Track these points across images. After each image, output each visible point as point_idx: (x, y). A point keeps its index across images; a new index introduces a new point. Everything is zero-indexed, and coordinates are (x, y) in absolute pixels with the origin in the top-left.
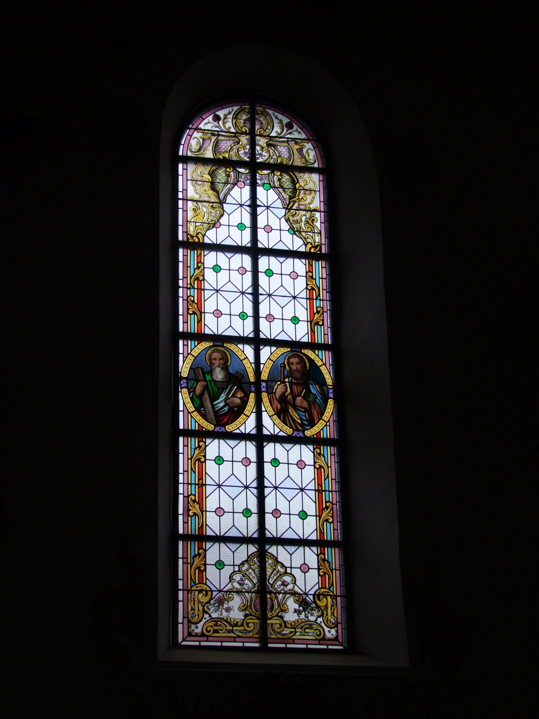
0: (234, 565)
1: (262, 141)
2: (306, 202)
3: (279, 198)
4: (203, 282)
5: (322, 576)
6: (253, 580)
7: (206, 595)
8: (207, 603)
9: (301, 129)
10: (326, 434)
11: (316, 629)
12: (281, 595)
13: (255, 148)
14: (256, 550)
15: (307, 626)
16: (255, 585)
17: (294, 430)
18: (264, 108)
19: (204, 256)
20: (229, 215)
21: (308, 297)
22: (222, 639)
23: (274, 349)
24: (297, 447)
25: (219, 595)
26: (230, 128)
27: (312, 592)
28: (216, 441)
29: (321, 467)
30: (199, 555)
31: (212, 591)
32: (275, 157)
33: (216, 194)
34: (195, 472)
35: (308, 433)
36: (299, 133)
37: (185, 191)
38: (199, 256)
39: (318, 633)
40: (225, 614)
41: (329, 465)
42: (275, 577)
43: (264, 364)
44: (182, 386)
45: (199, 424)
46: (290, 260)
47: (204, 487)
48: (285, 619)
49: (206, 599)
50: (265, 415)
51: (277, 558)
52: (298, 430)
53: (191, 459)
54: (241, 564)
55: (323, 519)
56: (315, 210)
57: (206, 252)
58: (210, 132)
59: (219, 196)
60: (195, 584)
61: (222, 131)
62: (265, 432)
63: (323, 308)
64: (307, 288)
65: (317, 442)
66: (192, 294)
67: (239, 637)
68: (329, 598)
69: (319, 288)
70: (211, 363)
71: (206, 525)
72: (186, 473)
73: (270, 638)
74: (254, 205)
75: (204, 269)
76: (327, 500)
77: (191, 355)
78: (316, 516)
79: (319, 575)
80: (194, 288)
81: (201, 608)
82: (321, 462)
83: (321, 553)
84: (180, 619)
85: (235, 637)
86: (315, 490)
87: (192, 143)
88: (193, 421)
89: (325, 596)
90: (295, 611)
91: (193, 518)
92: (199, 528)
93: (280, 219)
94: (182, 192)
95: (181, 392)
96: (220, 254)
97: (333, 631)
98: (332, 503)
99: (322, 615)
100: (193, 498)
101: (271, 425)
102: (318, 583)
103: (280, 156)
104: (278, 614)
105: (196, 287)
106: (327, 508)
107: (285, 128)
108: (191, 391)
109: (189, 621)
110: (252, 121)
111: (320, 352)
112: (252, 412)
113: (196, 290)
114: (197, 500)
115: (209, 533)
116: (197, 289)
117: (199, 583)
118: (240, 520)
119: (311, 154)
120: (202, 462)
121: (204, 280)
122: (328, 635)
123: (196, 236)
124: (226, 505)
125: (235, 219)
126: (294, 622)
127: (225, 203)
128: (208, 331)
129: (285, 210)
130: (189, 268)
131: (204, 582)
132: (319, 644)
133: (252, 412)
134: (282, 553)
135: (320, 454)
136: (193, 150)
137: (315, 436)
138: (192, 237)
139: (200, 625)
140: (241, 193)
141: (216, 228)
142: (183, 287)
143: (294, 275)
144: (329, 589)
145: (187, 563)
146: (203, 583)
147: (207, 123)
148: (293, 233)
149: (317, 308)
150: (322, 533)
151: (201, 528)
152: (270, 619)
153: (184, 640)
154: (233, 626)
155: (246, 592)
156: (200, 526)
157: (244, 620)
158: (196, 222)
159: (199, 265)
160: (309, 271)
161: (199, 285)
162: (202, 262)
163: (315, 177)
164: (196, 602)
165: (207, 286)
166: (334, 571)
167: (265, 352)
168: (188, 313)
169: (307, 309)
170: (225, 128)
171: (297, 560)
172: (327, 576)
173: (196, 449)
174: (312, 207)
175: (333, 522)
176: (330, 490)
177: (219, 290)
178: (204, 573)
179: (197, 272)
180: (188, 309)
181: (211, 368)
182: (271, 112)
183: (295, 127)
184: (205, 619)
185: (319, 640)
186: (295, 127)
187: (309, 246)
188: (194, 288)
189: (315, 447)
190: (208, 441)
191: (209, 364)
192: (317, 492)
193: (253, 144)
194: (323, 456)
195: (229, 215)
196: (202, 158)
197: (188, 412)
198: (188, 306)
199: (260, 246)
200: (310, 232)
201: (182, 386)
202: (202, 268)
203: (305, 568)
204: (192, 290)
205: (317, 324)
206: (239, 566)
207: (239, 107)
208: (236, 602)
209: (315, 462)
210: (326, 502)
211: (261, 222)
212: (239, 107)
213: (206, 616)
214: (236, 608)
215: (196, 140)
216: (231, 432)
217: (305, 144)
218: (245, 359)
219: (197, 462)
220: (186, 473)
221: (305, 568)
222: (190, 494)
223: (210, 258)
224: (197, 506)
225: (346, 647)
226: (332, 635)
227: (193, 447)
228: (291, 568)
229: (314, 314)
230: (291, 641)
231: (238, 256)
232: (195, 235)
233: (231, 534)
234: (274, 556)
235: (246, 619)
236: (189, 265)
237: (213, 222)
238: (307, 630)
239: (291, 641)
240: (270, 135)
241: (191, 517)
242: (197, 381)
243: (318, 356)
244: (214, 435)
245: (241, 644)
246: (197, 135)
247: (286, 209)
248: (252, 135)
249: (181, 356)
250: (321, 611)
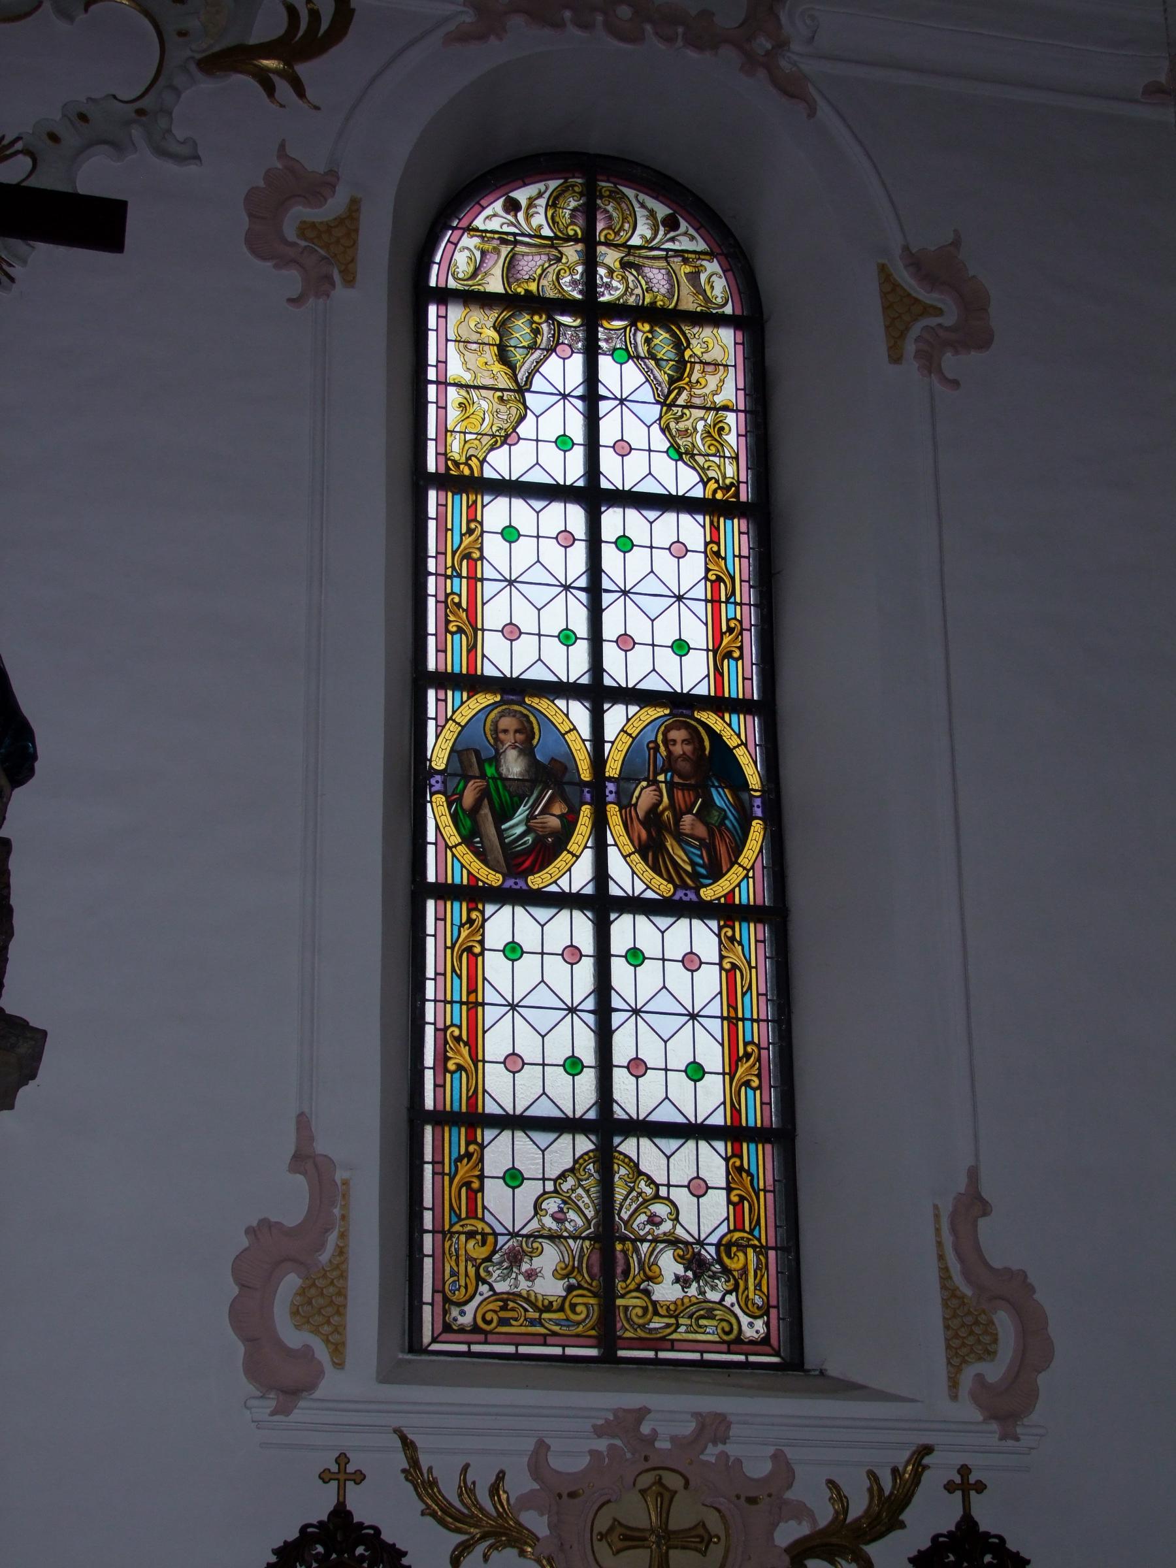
0: (544, 1179)
1: (610, 257)
2: (707, 391)
3: (647, 380)
4: (479, 563)
5: (736, 1205)
6: (586, 1212)
7: (484, 1243)
9: (697, 230)
10: (745, 896)
11: (722, 1320)
12: (646, 1245)
13: (596, 272)
14: (592, 1147)
16: (589, 1221)
17: (676, 887)
18: (615, 184)
19: (483, 506)
20: (537, 417)
21: (709, 597)
22: (517, 1339)
23: (633, 709)
24: (684, 923)
25: (510, 1243)
26: (540, 227)
27: (714, 1239)
28: (507, 909)
29: (734, 966)
30: (469, 1155)
31: (496, 1235)
32: (638, 291)
33: (509, 371)
34: (460, 977)
35: (707, 894)
36: (692, 238)
37: (441, 366)
38: (472, 507)
39: (727, 1329)
40: (524, 1285)
41: (753, 964)
42: (634, 1206)
43: (613, 743)
44: (433, 789)
45: (469, 873)
46: (670, 517)
47: (480, 1009)
48: (654, 1298)
49: (483, 1252)
50: (613, 854)
51: (637, 1165)
52: (685, 886)
55: (739, 1080)
56: (726, 408)
57: (487, 499)
58: (496, 236)
59: (515, 375)
61: (523, 235)
62: (614, 890)
63: (741, 622)
64: (706, 578)
65: (726, 913)
66: (456, 590)
67: (554, 1334)
68: (750, 1251)
69: (733, 579)
70: (497, 739)
71: (484, 1091)
72: (440, 979)
73: (620, 1338)
74: (591, 397)
75: (481, 535)
76: (748, 1038)
77: (454, 721)
78: (724, 1074)
79: (729, 1202)
80: (460, 576)
81: (472, 1271)
82: (735, 956)
83: (733, 1155)
84: (427, 1296)
85: (545, 1336)
86: (722, 1018)
87: (457, 259)
88: (457, 866)
89: (743, 1248)
90: (677, 1279)
91: (457, 1075)
92: (468, 1098)
93: (649, 427)
94: (436, 366)
95: (431, 802)
96: (518, 503)
97: (759, 1324)
98: (758, 1046)
100: (457, 1033)
101: (625, 877)
102: (728, 1218)
103: (649, 290)
104: (639, 1285)
105: (464, 574)
106: (748, 1056)
107: (662, 229)
108: (453, 800)
109: (446, 1300)
110: (589, 212)
111: (734, 717)
112: (586, 847)
113: (464, 581)
114: (465, 1037)
115: (491, 1108)
116: (467, 578)
117: (467, 1217)
118: (558, 1081)
119: (717, 285)
120: (476, 956)
121: (482, 558)
122: (749, 1333)
123: (466, 464)
124: (529, 1048)
125: (551, 427)
126: (675, 1303)
127: (529, 390)
128: (490, 671)
129: (659, 407)
130: (449, 533)
131: (480, 1215)
132: (729, 1352)
133: (586, 847)
134: (648, 1154)
135: (732, 939)
136: (461, 276)
137: (722, 900)
138: (457, 464)
139: (470, 1308)
140: (564, 371)
141: (510, 445)
142: (436, 574)
143: (679, 550)
144: (751, 1232)
145: (443, 1174)
146: (476, 1217)
147: (492, 217)
148: (677, 457)
149: (728, 620)
150: (736, 1111)
151: (472, 1099)
152: (623, 1296)
153: (434, 1340)
154: (541, 1312)
157: (565, 1298)
158: (465, 433)
159: (473, 526)
160: (712, 542)
161: (472, 569)
162: (479, 519)
163: (727, 335)
164: (462, 1258)
165: (489, 572)
166: (762, 1194)
167: (615, 717)
168: (447, 631)
169: (706, 624)
170: (531, 228)
171: (682, 1170)
172: (746, 1204)
173: (462, 925)
174: (719, 400)
175: (760, 1087)
176: (755, 1017)
177: (515, 581)
178: (479, 1195)
179: (467, 540)
180: (448, 622)
181: (497, 750)
182: (630, 193)
183: (684, 225)
184: (481, 1294)
185: (729, 1343)
186: (684, 225)
187: (712, 485)
188: (460, 576)
189: (722, 923)
190: (490, 909)
191: (492, 741)
192: (725, 1023)
193: (590, 262)
194: (740, 943)
195: (537, 417)
196: (479, 292)
197: (447, 846)
198: (447, 615)
199: (604, 484)
200: (714, 455)
201: (433, 789)
202: (478, 532)
203: (698, 1187)
204: (456, 581)
205: (728, 655)
206: (555, 1181)
207: (561, 181)
208: (549, 1258)
209: (722, 957)
210: (746, 1044)
211: (608, 432)
212: (561, 181)
213: (484, 1288)
214: (548, 1272)
215: (467, 253)
216: (539, 890)
217: (704, 263)
218: (571, 730)
219: (465, 955)
220: (440, 979)
221: (698, 1187)
222: (448, 1023)
223: (497, 512)
224: (465, 1051)
226: (757, 1332)
227: (457, 922)
228: (669, 1186)
229: (722, 634)
230: (668, 1345)
231: (557, 508)
232: (463, 460)
233: (537, 1111)
234: (631, 1160)
235: (570, 1297)
236: (449, 526)
237: (503, 433)
238: (702, 1322)
240: (630, 243)
241: (452, 1073)
242: (467, 778)
243: (730, 725)
244: (502, 896)
245: (558, 1351)
246: (469, 241)
247: (663, 404)
248: (590, 242)
249: (431, 725)
250: (732, 1281)
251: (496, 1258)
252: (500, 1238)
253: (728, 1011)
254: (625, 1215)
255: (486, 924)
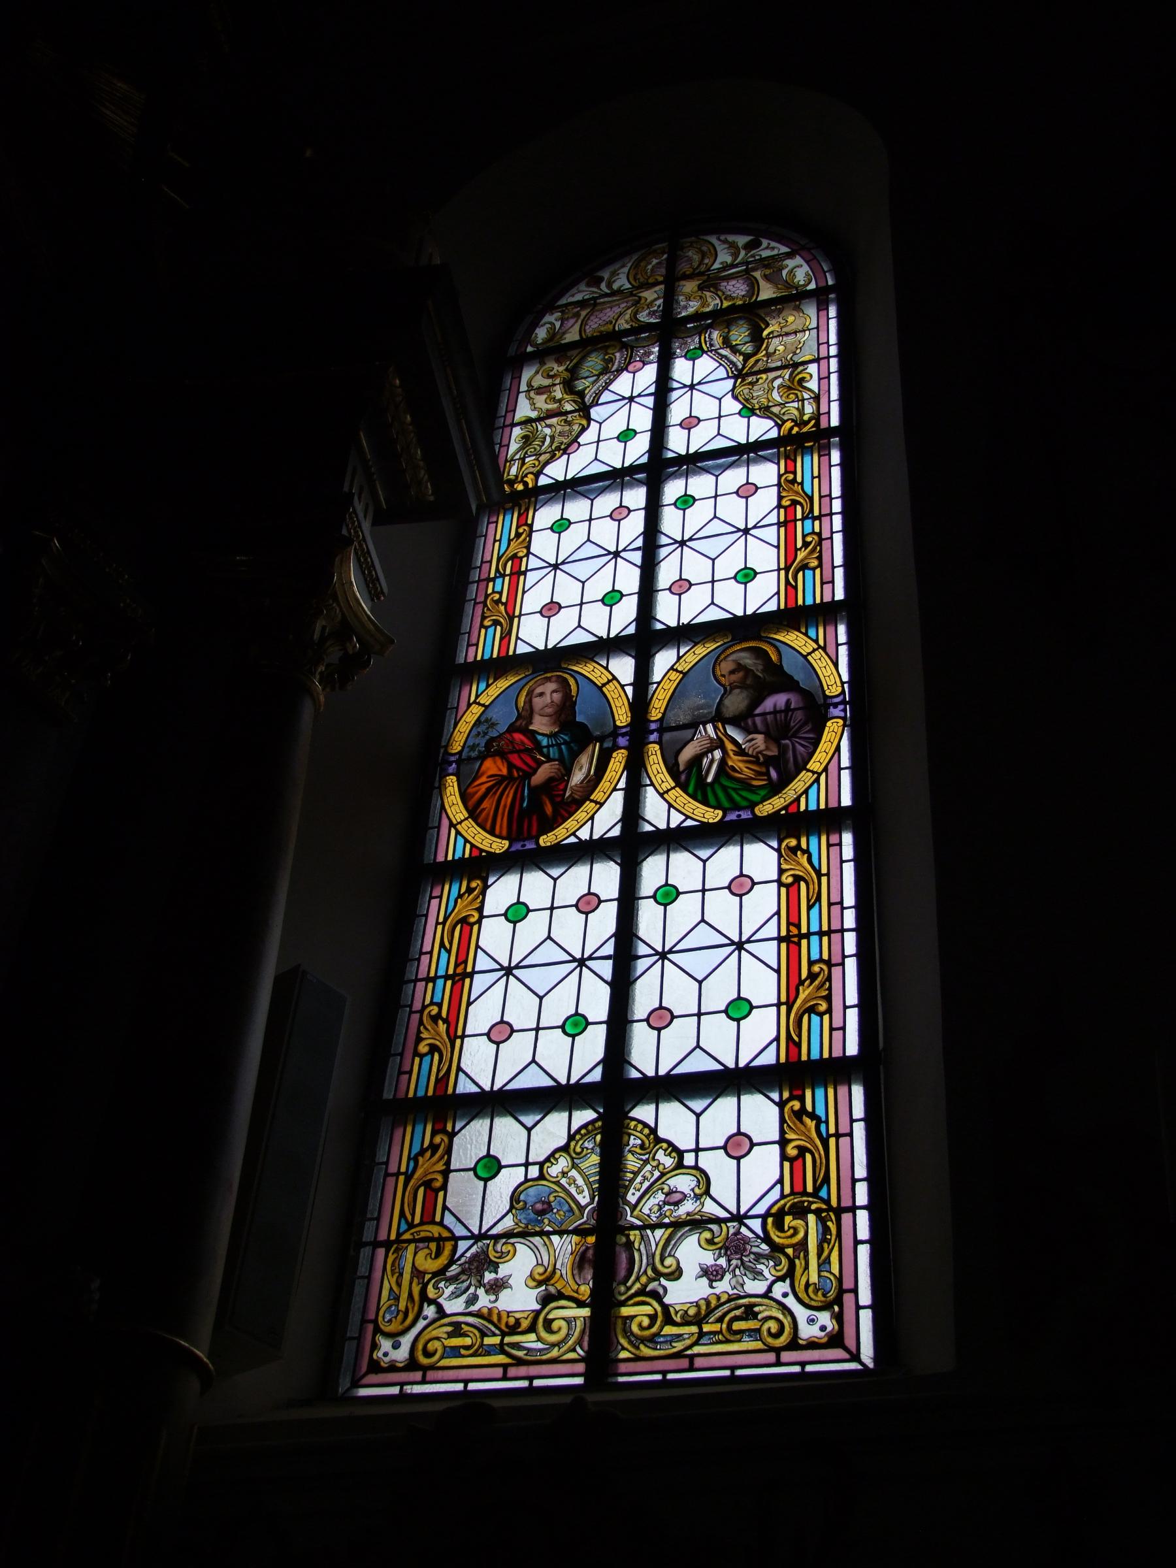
5: (792, 1160)
6: (579, 1198)
7: (438, 1254)
8: (435, 1274)
12: (659, 1233)
15: (737, 1312)
22: (464, 1374)
27: (761, 1209)
30: (434, 1148)
31: (456, 1239)
34: (449, 952)
39: (773, 1331)
40: (484, 1301)
41: (824, 870)
42: (646, 1184)
48: (667, 1300)
49: (433, 1265)
51: (654, 1131)
52: (737, 807)
53: (444, 923)
54: (547, 1160)
60: (411, 1226)
64: (779, 506)
67: (520, 1362)
68: (811, 1218)
75: (530, 536)
78: (778, 1005)
79: (784, 1157)
81: (416, 1290)
85: (505, 1366)
98: (829, 964)
99: (790, 1274)
102: (780, 1181)
104: (646, 1286)
112: (615, 789)
113: (507, 579)
117: (422, 1223)
122: (807, 1332)
126: (697, 1305)
130: (497, 544)
134: (673, 1120)
139: (406, 1341)
144: (815, 1194)
146: (433, 1222)
150: (793, 1044)
154: (504, 1334)
155: (555, 1233)
156: (441, 1074)
157: (537, 1313)
166: (832, 1141)
184: (425, 1318)
185: (777, 1351)
187: (789, 425)
205: (804, 567)
206: (541, 1164)
209: (781, 871)
210: (811, 963)
213: (430, 1311)
218: (609, 681)
221: (738, 1145)
222: (427, 1001)
225: (871, 1366)
226: (823, 1328)
229: (797, 550)
234: (646, 1125)
238: (737, 1326)
239: (685, 1363)
251: (454, 1269)
252: (460, 1243)
253: (788, 930)
254: (632, 1198)
255: (488, 891)
